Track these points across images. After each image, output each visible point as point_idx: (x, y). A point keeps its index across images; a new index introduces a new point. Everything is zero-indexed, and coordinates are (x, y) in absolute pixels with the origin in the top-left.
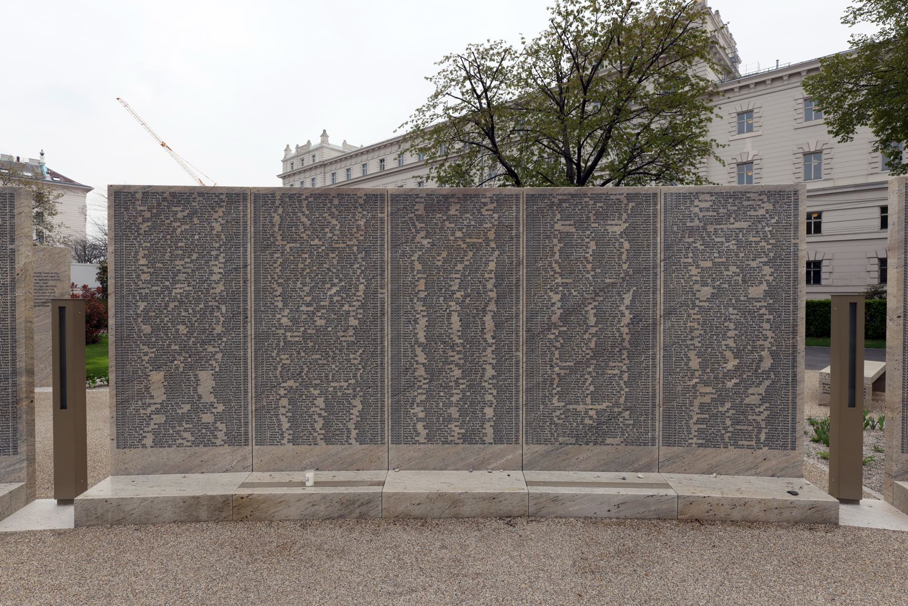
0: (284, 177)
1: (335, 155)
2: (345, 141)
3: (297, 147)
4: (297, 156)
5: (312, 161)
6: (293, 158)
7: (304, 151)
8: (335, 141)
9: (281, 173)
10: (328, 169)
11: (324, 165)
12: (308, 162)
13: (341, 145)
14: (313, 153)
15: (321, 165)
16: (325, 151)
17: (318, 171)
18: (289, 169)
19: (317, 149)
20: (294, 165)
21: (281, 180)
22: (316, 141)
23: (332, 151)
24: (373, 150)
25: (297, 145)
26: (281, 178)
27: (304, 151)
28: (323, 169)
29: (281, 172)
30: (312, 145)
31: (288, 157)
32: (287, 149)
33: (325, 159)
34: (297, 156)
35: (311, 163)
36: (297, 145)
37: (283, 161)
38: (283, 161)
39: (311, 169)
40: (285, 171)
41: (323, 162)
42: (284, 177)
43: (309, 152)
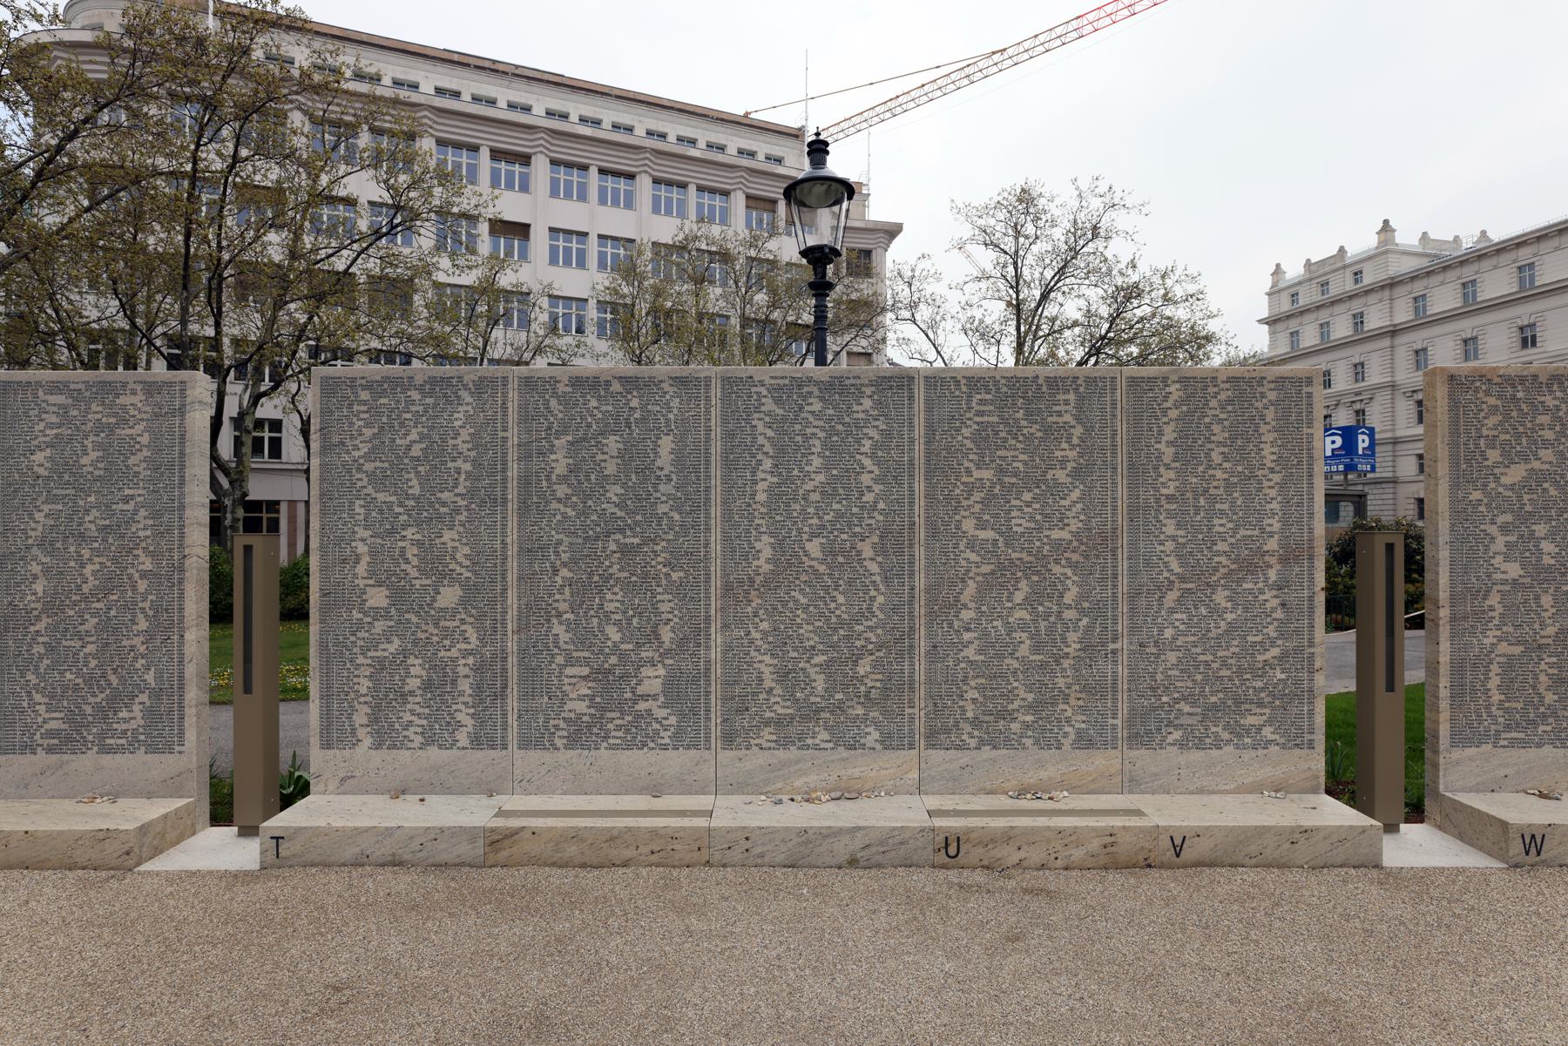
0: (1271, 322)
1: (1407, 266)
2: (1425, 234)
3: (1308, 263)
4: (1311, 280)
5: (1352, 281)
6: (1300, 283)
7: (1318, 273)
8: (1406, 237)
9: (1266, 315)
10: (1400, 291)
11: (1392, 284)
12: (1342, 284)
13: (1417, 243)
14: (1356, 268)
15: (1382, 287)
16: (1391, 257)
17: (1372, 298)
18: (1286, 306)
19: (1370, 258)
20: (1300, 297)
21: (1266, 327)
22: (1361, 241)
23: (1404, 259)
24: (1539, 239)
25: (1308, 260)
26: (1267, 323)
27: (1328, 269)
28: (1386, 293)
29: (1266, 315)
30: (1349, 255)
31: (1281, 285)
32: (1278, 271)
33: (1391, 273)
34: (1311, 280)
35: (1349, 286)
36: (1308, 260)
37: (1269, 294)
38: (1269, 294)
39: (1351, 297)
40: (1276, 311)
41: (1392, 278)
42: (1271, 322)
43: (1345, 267)
